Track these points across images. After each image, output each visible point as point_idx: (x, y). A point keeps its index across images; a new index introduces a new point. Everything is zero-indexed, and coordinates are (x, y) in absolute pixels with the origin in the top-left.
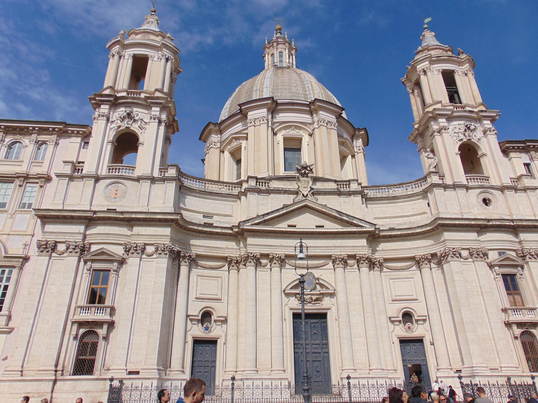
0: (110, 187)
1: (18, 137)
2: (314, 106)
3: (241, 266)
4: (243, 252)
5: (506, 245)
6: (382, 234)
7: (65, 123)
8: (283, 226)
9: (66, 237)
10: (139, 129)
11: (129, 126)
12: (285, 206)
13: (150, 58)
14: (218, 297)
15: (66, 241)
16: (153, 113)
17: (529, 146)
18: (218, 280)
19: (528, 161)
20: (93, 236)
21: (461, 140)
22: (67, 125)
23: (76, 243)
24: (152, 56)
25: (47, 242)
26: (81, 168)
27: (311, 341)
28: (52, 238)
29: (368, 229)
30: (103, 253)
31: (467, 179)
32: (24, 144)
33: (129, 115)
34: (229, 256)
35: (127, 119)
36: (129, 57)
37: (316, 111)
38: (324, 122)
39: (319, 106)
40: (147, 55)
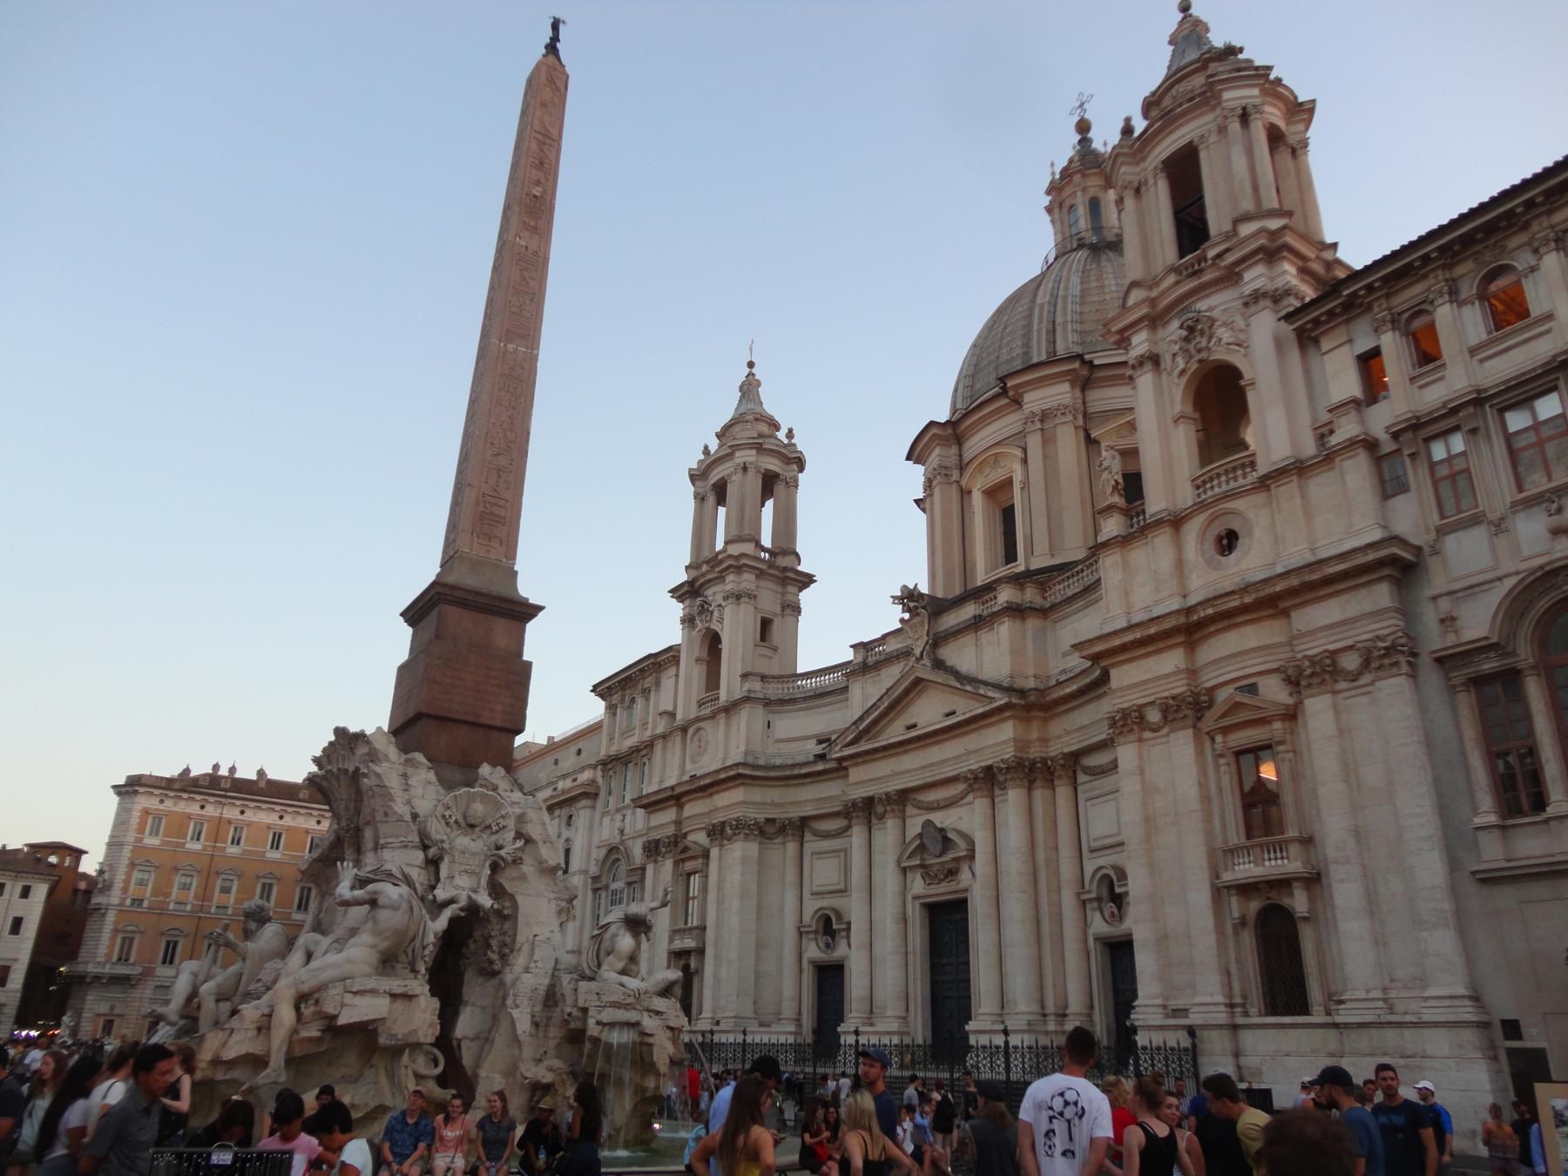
5: (1225, 670)
6: (1048, 699)
8: (895, 732)
12: (888, 690)
14: (842, 886)
16: (728, 587)
17: (1354, 295)
18: (839, 857)
19: (1364, 345)
21: (1183, 372)
23: (668, 837)
24: (728, 475)
25: (649, 842)
27: (957, 957)
29: (998, 703)
30: (686, 849)
31: (1198, 487)
33: (704, 609)
37: (1021, 395)
38: (1033, 422)
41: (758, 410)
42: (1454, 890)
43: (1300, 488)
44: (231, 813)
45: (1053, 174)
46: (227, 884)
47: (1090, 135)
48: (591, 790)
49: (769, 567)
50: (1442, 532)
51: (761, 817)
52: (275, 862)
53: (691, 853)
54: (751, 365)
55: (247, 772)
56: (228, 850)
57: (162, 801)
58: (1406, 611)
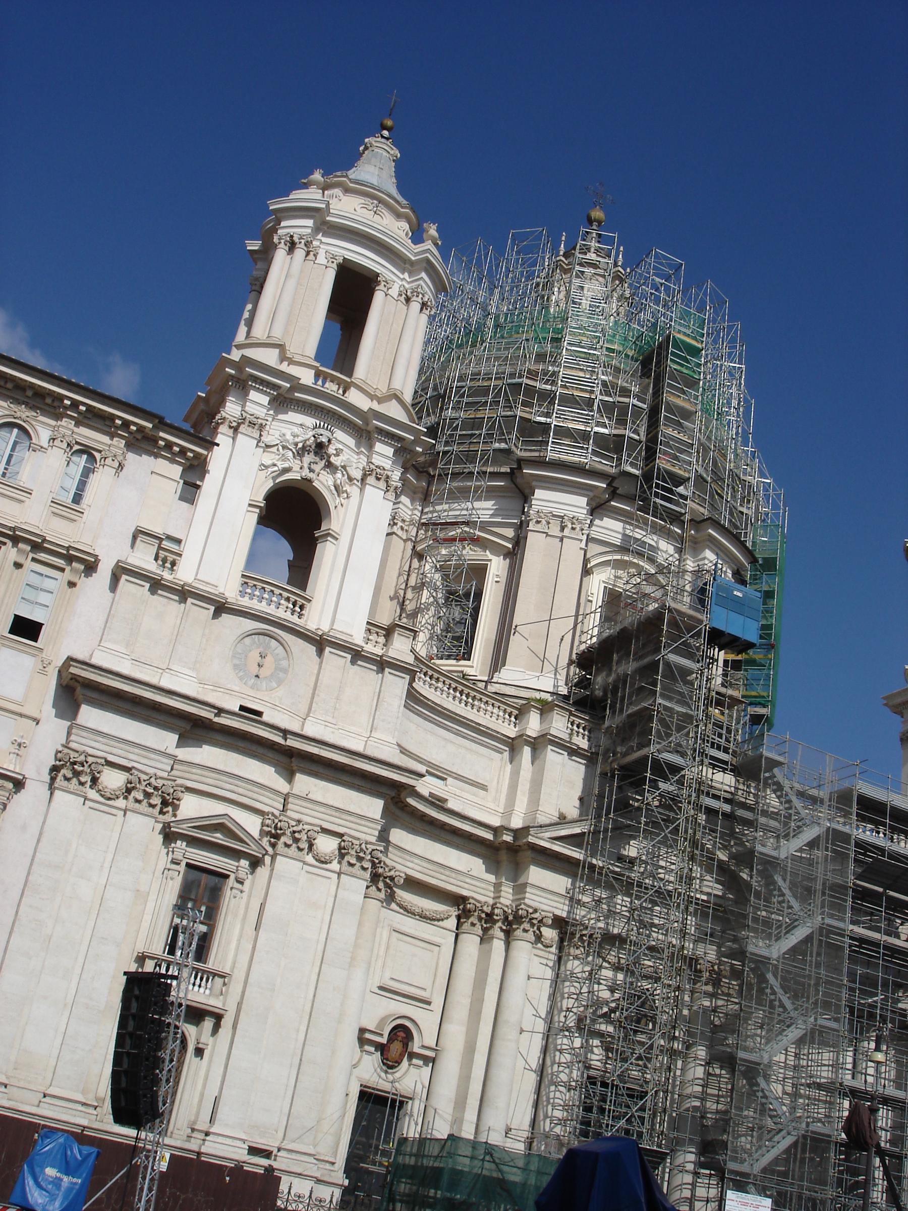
0: (248, 641)
1: (23, 413)
2: (697, 531)
3: (497, 931)
4: (507, 898)
9: (132, 756)
10: (335, 492)
11: (311, 475)
13: (381, 287)
15: (133, 767)
16: (377, 460)
20: (194, 771)
22: (161, 423)
25: (87, 755)
26: (171, 557)
28: (97, 748)
32: (34, 441)
34: (473, 898)
35: (312, 454)
36: (330, 264)
39: (712, 539)
40: (378, 275)
53: (218, 838)
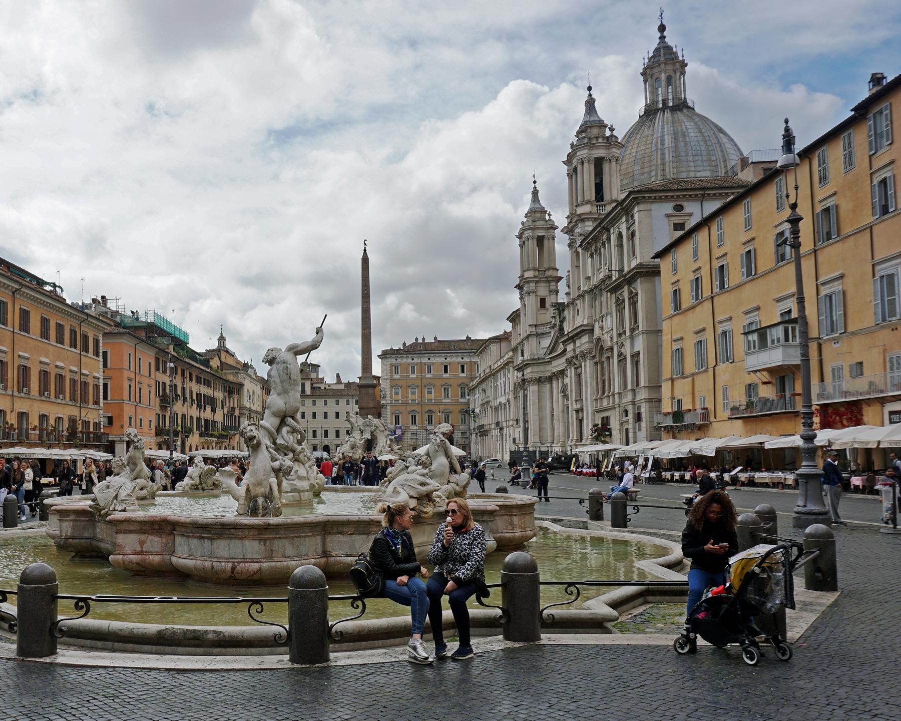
7: (514, 312)
21: (574, 252)
41: (537, 206)
42: (593, 415)
43: (583, 301)
44: (425, 360)
45: (644, 64)
46: (429, 390)
47: (665, 34)
48: (510, 360)
49: (540, 278)
50: (595, 321)
51: (537, 376)
52: (447, 378)
54: (535, 182)
55: (430, 339)
56: (427, 376)
57: (396, 360)
58: (591, 341)
